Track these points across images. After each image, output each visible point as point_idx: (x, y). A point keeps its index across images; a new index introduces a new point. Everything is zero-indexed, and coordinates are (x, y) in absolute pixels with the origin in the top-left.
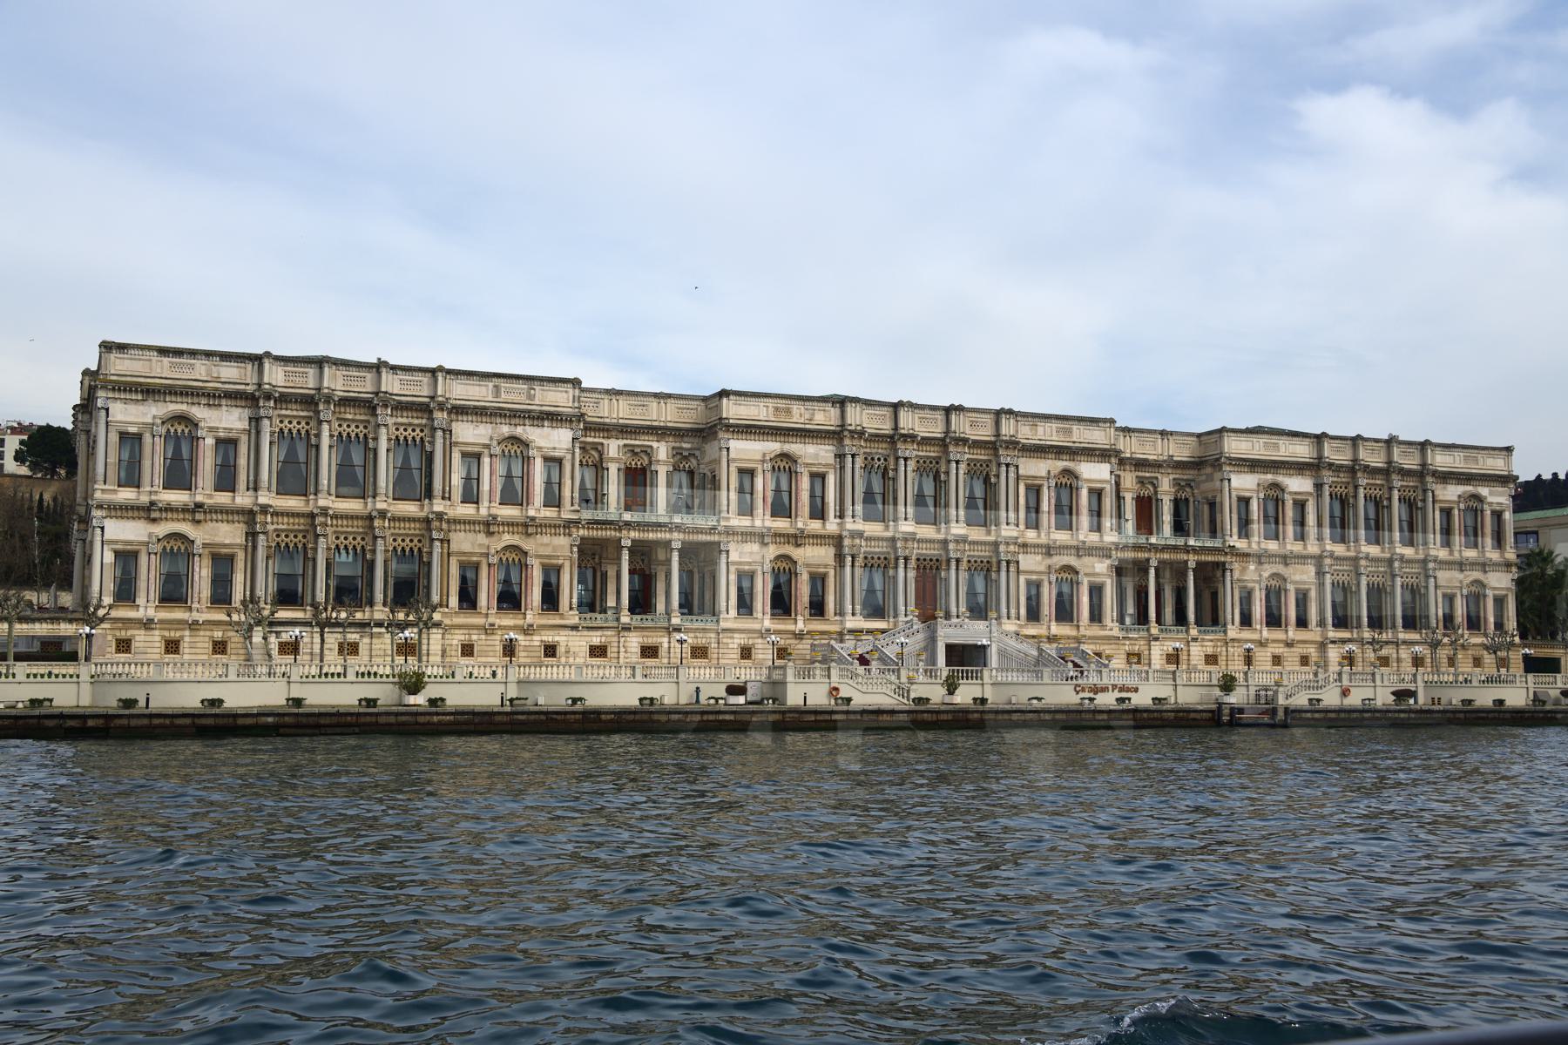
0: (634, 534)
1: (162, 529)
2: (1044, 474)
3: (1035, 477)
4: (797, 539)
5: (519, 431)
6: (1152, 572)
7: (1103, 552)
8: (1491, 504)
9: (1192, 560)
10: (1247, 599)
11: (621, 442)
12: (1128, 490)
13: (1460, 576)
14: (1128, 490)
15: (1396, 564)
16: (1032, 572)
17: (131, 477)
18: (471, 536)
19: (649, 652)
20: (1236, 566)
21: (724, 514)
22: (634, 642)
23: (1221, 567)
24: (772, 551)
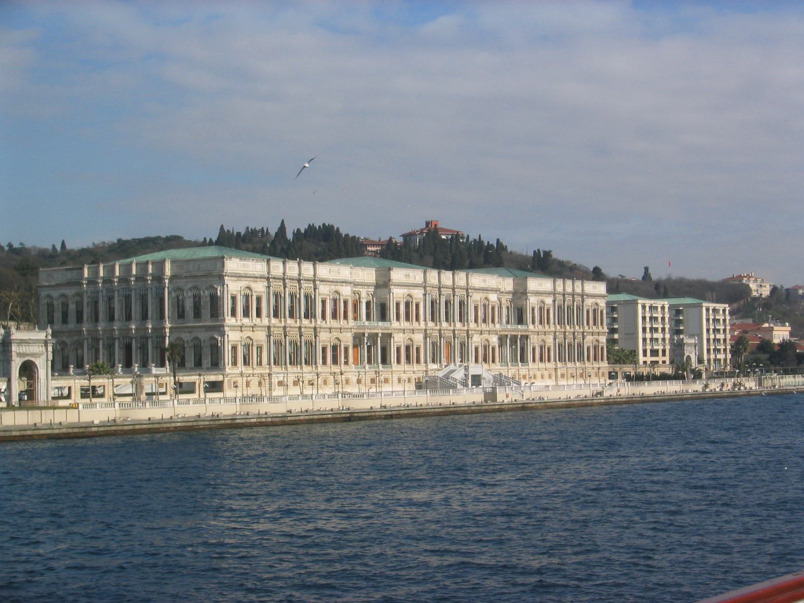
0: (368, 331)
2: (479, 299)
4: (413, 331)
7: (496, 332)
20: (531, 336)
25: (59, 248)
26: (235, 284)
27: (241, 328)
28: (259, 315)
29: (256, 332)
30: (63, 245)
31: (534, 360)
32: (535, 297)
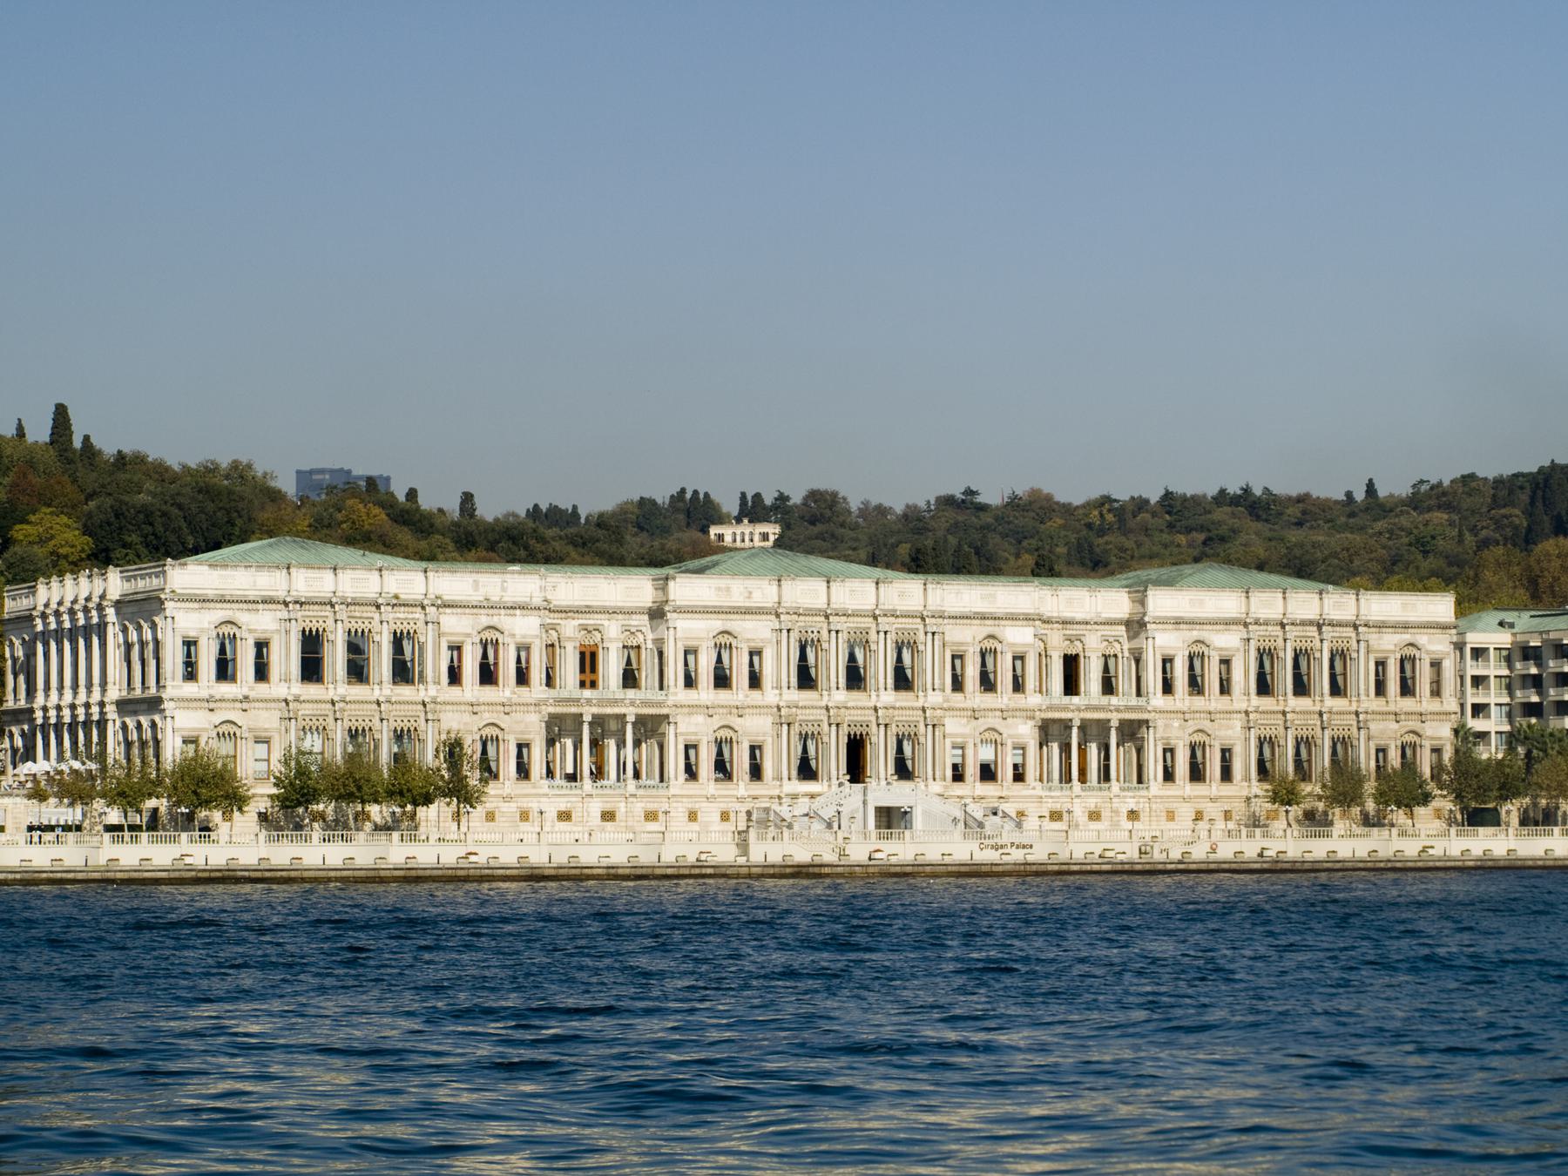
0: (595, 710)
1: (218, 718)
3: (962, 644)
5: (495, 621)
6: (1075, 731)
8: (1428, 652)
10: (1169, 751)
11: (576, 622)
12: (1054, 648)
13: (1395, 726)
14: (1054, 648)
15: (1325, 717)
16: (956, 735)
17: (191, 674)
18: (457, 715)
19: (608, 816)
20: (1160, 723)
21: (672, 689)
22: (596, 807)
23: (1145, 723)
24: (717, 722)
25: (1360, 495)
26: (194, 616)
27: (210, 704)
28: (262, 673)
29: (251, 713)
30: (1371, 488)
31: (1169, 776)
32: (1177, 634)
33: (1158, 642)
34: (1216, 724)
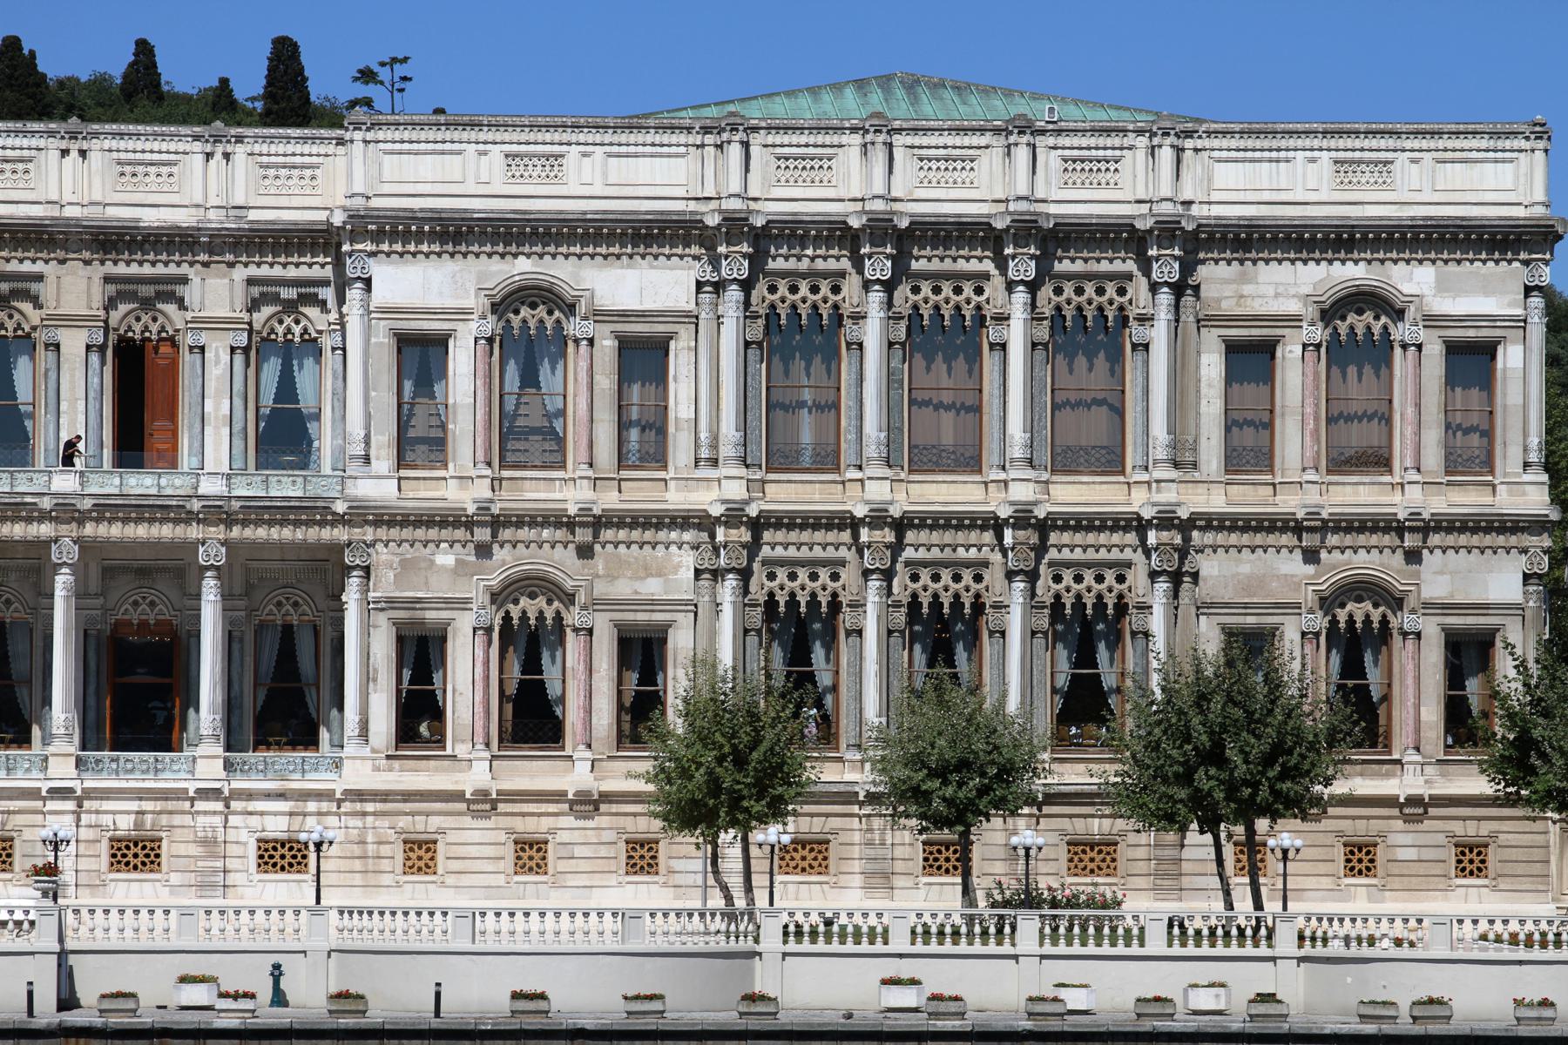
8: (1432, 321)
9: (211, 544)
10: (421, 652)
12: (71, 321)
14: (71, 321)
33: (380, 296)
34: (599, 564)
